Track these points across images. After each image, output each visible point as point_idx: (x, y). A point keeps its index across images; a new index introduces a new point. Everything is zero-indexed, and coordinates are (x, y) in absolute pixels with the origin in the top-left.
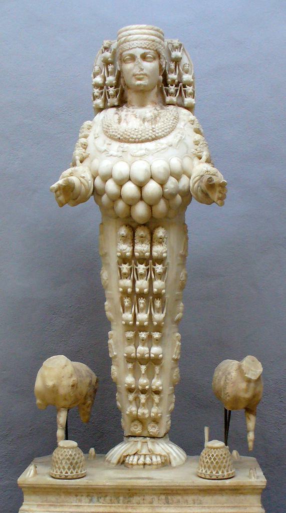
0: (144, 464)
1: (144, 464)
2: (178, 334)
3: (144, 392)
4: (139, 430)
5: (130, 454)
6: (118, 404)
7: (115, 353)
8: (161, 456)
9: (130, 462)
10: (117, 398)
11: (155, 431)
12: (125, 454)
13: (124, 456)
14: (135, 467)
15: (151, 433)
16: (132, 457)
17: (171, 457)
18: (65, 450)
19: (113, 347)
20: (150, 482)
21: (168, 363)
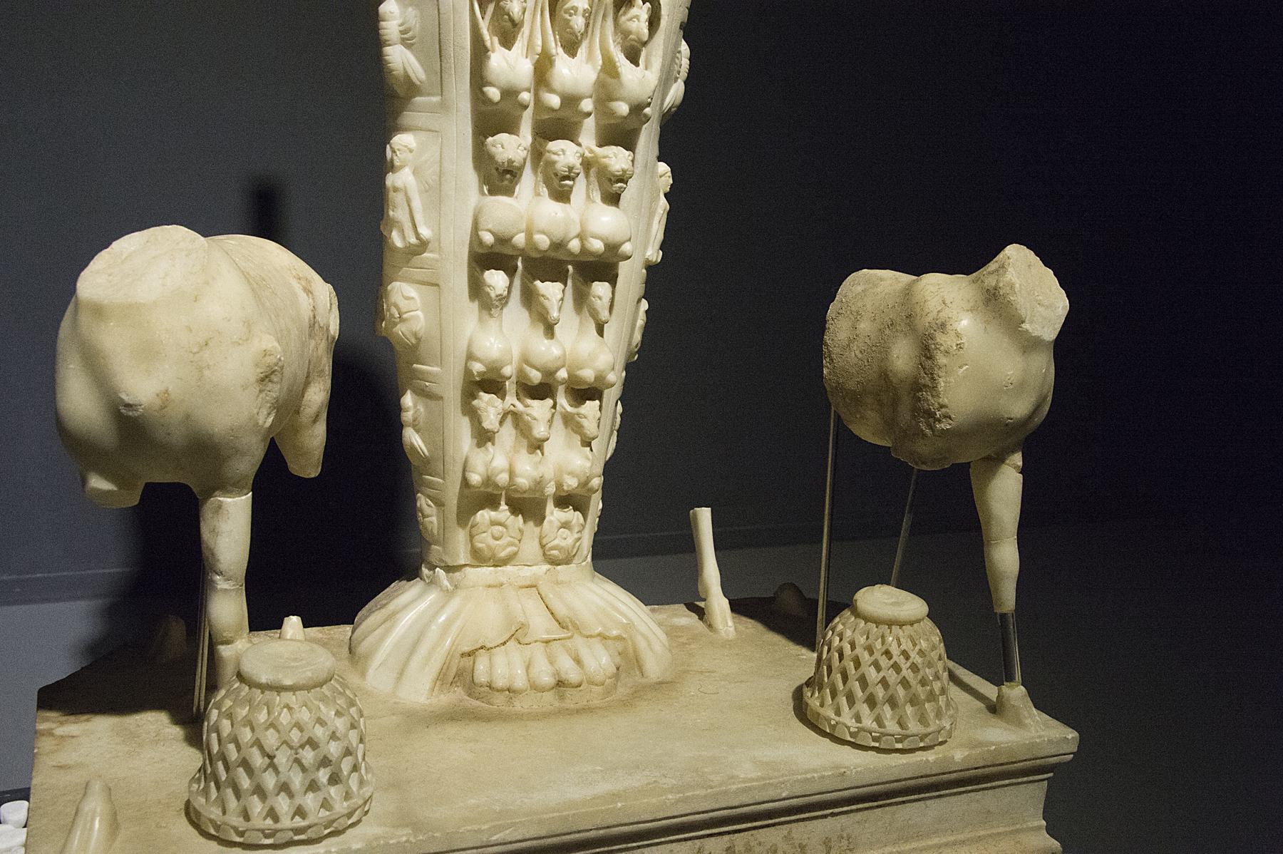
0: (560, 684)
1: (560, 684)
2: (663, 168)
3: (541, 391)
4: (512, 544)
5: (489, 645)
6: (413, 438)
7: (425, 232)
8: (603, 637)
9: (500, 683)
10: (407, 416)
11: (570, 541)
12: (466, 649)
13: (463, 655)
14: (519, 706)
15: (555, 552)
16: (500, 658)
17: (642, 644)
18: (289, 698)
19: (417, 204)
20: (678, 801)
21: (631, 275)
